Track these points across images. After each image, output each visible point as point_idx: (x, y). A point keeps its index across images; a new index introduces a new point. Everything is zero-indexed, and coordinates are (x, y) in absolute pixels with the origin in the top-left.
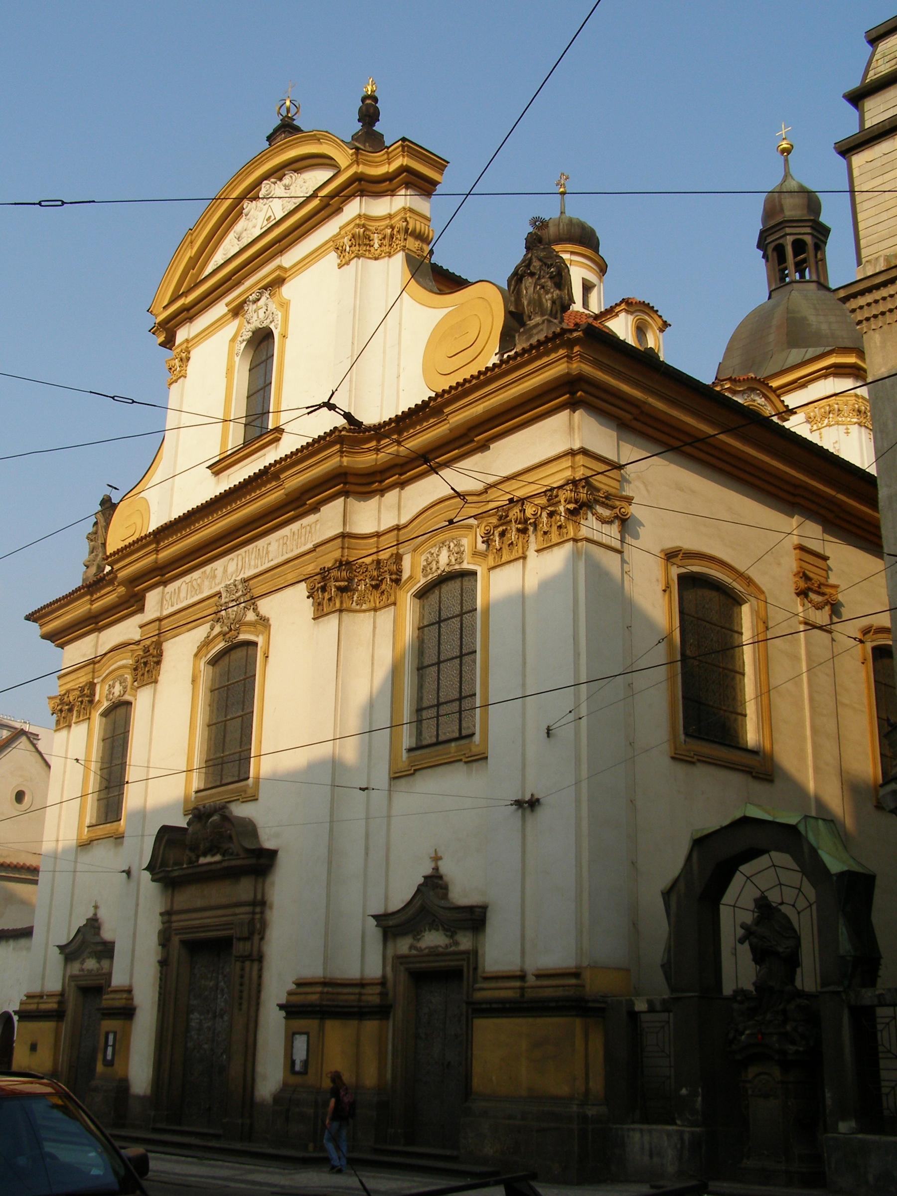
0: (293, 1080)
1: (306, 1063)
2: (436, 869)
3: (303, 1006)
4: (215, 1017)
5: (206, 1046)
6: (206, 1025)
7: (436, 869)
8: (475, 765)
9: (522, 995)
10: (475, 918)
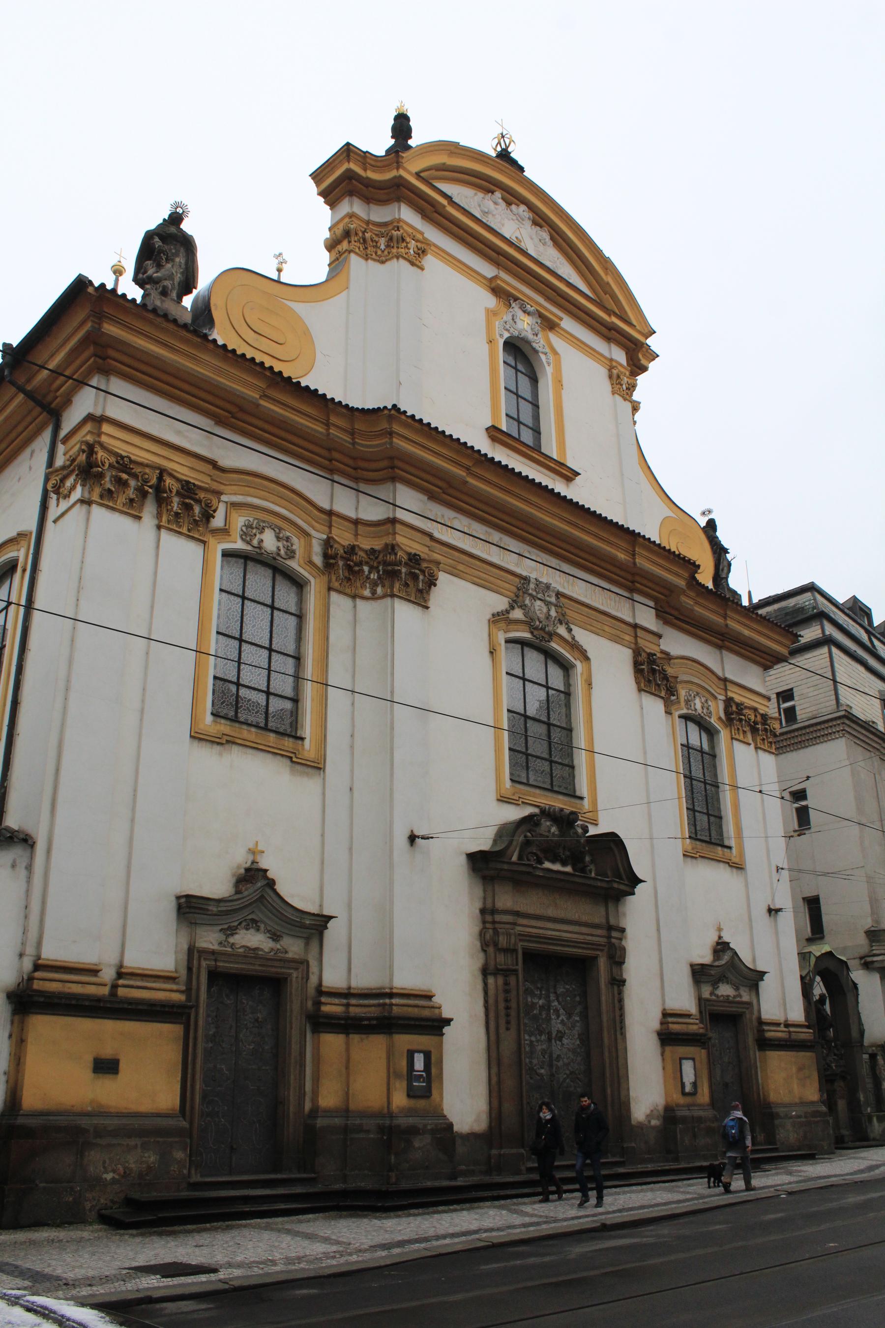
1: (695, 1084)
2: (720, 937)
3: (683, 1034)
5: (542, 1071)
6: (539, 1048)
7: (720, 937)
8: (735, 870)
9: (790, 1037)
10: (754, 979)
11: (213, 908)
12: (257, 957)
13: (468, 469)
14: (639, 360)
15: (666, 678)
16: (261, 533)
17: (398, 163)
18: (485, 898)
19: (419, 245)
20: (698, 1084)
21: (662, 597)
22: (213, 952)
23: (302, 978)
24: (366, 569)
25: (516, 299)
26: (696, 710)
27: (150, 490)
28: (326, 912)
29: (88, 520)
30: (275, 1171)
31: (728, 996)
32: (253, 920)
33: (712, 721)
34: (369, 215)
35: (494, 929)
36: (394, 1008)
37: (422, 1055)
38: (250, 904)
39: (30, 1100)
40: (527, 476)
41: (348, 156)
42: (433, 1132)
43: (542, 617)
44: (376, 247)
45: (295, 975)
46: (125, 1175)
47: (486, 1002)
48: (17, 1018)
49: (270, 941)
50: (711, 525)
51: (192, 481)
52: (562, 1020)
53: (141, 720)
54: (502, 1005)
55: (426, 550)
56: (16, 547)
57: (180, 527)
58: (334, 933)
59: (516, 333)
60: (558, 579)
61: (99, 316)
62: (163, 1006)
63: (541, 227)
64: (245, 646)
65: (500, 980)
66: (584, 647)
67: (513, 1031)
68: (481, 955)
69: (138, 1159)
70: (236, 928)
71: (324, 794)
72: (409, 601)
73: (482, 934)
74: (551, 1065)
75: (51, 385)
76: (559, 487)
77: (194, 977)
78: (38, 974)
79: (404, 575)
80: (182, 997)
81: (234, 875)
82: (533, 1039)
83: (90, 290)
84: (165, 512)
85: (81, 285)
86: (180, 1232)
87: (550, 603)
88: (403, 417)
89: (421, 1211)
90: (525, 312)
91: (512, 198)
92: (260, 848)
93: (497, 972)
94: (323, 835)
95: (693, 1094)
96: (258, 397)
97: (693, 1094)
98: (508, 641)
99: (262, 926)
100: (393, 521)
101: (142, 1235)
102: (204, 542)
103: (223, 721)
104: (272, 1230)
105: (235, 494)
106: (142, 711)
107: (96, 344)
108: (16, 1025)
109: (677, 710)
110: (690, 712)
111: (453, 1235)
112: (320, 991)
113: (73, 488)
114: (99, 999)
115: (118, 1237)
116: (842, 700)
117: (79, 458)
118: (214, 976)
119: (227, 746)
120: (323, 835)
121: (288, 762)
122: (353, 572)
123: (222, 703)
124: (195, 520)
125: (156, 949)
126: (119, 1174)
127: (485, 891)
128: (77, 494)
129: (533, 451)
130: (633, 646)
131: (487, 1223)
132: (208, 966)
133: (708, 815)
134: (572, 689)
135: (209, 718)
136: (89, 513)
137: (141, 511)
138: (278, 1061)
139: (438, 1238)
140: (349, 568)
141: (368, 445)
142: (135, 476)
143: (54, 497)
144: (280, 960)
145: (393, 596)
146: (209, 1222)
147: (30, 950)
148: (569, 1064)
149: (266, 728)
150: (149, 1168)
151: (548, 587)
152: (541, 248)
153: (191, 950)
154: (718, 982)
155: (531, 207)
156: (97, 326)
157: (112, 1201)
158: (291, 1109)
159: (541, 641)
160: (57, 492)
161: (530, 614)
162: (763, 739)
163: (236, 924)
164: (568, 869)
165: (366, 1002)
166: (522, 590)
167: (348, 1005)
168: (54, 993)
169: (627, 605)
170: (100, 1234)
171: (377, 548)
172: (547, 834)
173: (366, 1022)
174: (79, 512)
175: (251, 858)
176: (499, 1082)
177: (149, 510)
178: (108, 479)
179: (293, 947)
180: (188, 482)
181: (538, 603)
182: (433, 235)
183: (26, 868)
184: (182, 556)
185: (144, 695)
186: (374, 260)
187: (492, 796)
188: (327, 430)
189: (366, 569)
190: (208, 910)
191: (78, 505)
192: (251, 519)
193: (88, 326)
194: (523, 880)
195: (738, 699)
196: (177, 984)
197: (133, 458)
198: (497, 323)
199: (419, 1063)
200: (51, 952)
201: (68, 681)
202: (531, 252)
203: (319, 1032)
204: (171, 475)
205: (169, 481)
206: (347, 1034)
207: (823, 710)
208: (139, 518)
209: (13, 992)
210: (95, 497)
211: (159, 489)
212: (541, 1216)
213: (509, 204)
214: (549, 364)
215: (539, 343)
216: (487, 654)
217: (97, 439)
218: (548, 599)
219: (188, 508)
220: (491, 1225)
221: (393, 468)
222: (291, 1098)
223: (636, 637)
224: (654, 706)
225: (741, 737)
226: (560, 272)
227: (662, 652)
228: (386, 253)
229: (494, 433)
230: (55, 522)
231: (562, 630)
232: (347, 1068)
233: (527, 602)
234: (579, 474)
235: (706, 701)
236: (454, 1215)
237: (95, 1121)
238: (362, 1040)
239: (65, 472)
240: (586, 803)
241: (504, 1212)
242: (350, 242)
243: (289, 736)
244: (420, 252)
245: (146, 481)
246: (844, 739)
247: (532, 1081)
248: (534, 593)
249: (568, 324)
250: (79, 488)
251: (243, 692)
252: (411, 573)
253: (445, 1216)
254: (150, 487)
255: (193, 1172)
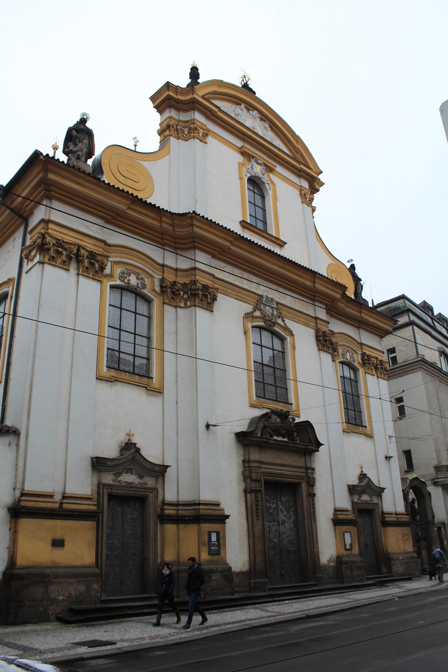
0: (345, 553)
1: (351, 545)
2: (362, 471)
4: (279, 524)
5: (275, 540)
7: (362, 471)
8: (368, 438)
11: (110, 464)
12: (132, 487)
13: (231, 242)
14: (315, 186)
15: (332, 343)
16: (129, 276)
17: (193, 91)
18: (244, 455)
19: (204, 131)
20: (353, 544)
21: (329, 303)
22: (110, 485)
23: (155, 497)
24: (182, 293)
25: (253, 157)
26: (347, 359)
27: (73, 256)
28: (165, 464)
29: (43, 271)
30: (144, 593)
31: (367, 500)
32: (129, 469)
33: (355, 364)
34: (179, 117)
35: (250, 471)
36: (201, 510)
37: (215, 534)
38: (128, 461)
39: (20, 561)
40: (261, 245)
41: (168, 88)
42: (222, 572)
43: (270, 314)
44: (183, 133)
45: (151, 495)
46: (69, 597)
47: (246, 506)
48: (13, 520)
49: (138, 479)
50: (353, 267)
51: (94, 251)
52: (285, 515)
53: (72, 370)
54: (254, 508)
55: (211, 283)
56: (7, 286)
57: (89, 274)
58: (170, 474)
59: (254, 174)
60: (277, 296)
61: (46, 171)
62: (86, 512)
63: (265, 121)
64: (122, 333)
65: (253, 496)
66: (291, 329)
67: (260, 521)
68: (244, 483)
69: (77, 589)
70: (121, 473)
71: (163, 405)
72: (203, 308)
73: (243, 473)
74: (279, 537)
75: (23, 205)
76: (277, 250)
77: (101, 497)
78: (23, 498)
79: (201, 295)
80: (95, 508)
81: (119, 447)
82: (270, 524)
83: (41, 157)
84: (81, 266)
85: (37, 155)
86: (97, 625)
87: (274, 307)
88: (198, 217)
89: (216, 611)
90: (257, 163)
91: (250, 107)
92: (132, 433)
93: (251, 491)
94: (163, 426)
95: (351, 549)
96: (126, 208)
97: (351, 549)
98: (253, 327)
99: (134, 472)
100: (195, 269)
101: (78, 627)
102: (101, 281)
103: (112, 370)
104: (143, 622)
105: (116, 257)
106: (72, 366)
107: (45, 184)
108: (12, 524)
109: (338, 359)
110: (344, 360)
111: (233, 623)
112: (164, 503)
113: (35, 256)
114: (53, 510)
115: (66, 628)
116: (420, 352)
117: (38, 241)
118: (111, 497)
119: (115, 383)
120: (163, 426)
121: (145, 389)
122: (175, 294)
123: (112, 361)
124: (96, 271)
125: (82, 484)
126: (66, 597)
127: (244, 451)
128: (37, 259)
129: (263, 233)
130: (315, 328)
131: (250, 616)
132: (108, 492)
133: (355, 411)
134: (285, 350)
135: (105, 369)
136: (43, 268)
137: (69, 266)
138: (144, 538)
139: (225, 624)
140: (173, 293)
141: (180, 232)
142: (66, 249)
143: (26, 260)
144: (143, 488)
145: (195, 306)
146: (111, 619)
147: (19, 486)
148: (288, 536)
149: (134, 373)
150: (81, 593)
151: (272, 299)
152: (265, 132)
153: (99, 485)
154: (361, 494)
155: (260, 112)
156: (45, 175)
157: (63, 610)
158: (151, 562)
159: (269, 326)
160: (27, 258)
161: (264, 313)
162: (381, 373)
163: (121, 471)
164: (286, 439)
165: (187, 508)
166: (259, 301)
167: (178, 510)
168: (31, 507)
169: (312, 308)
170: (57, 627)
171: (187, 282)
172: (275, 422)
173: (187, 518)
174: (38, 268)
175: (128, 438)
176: (254, 546)
177: (73, 266)
178: (52, 251)
179: (150, 482)
180: (92, 252)
181: (268, 308)
182: (211, 126)
183: (16, 445)
184: (90, 288)
185: (72, 358)
186: (181, 139)
187: (247, 404)
188: (161, 224)
189: (182, 293)
190: (107, 464)
191: (38, 264)
192: (124, 269)
193: (41, 175)
194: (263, 446)
195: (368, 353)
196: (93, 501)
197: (64, 240)
198: (244, 169)
199: (214, 538)
200: (29, 487)
201: (35, 352)
202: (260, 134)
203: (164, 524)
204: (84, 249)
205: (82, 251)
206: (178, 524)
207: (411, 357)
208: (68, 270)
209: (11, 507)
210: (46, 260)
211: (78, 255)
212: (276, 612)
213: (248, 110)
214: (270, 189)
215: (265, 179)
216: (243, 334)
217: (46, 231)
218: (272, 305)
219: (92, 264)
220: (252, 617)
221: (194, 242)
222: (151, 556)
223: (317, 323)
224: (327, 358)
225: (370, 372)
226: (275, 144)
227: (330, 331)
228: (188, 136)
229: (243, 224)
230: (26, 273)
231: (280, 321)
232: (178, 541)
233: (262, 307)
234: (286, 243)
235: (352, 354)
236: (233, 612)
237: (53, 570)
238: (185, 527)
239: (31, 248)
240: (294, 406)
241: (258, 611)
242: (170, 131)
243: (145, 377)
244: (205, 135)
245: (71, 252)
246: (421, 371)
247: (270, 545)
248: (266, 303)
249: (279, 169)
250: (38, 256)
251: (122, 355)
252: (204, 294)
253: (229, 614)
254: (73, 254)
255: (103, 594)
